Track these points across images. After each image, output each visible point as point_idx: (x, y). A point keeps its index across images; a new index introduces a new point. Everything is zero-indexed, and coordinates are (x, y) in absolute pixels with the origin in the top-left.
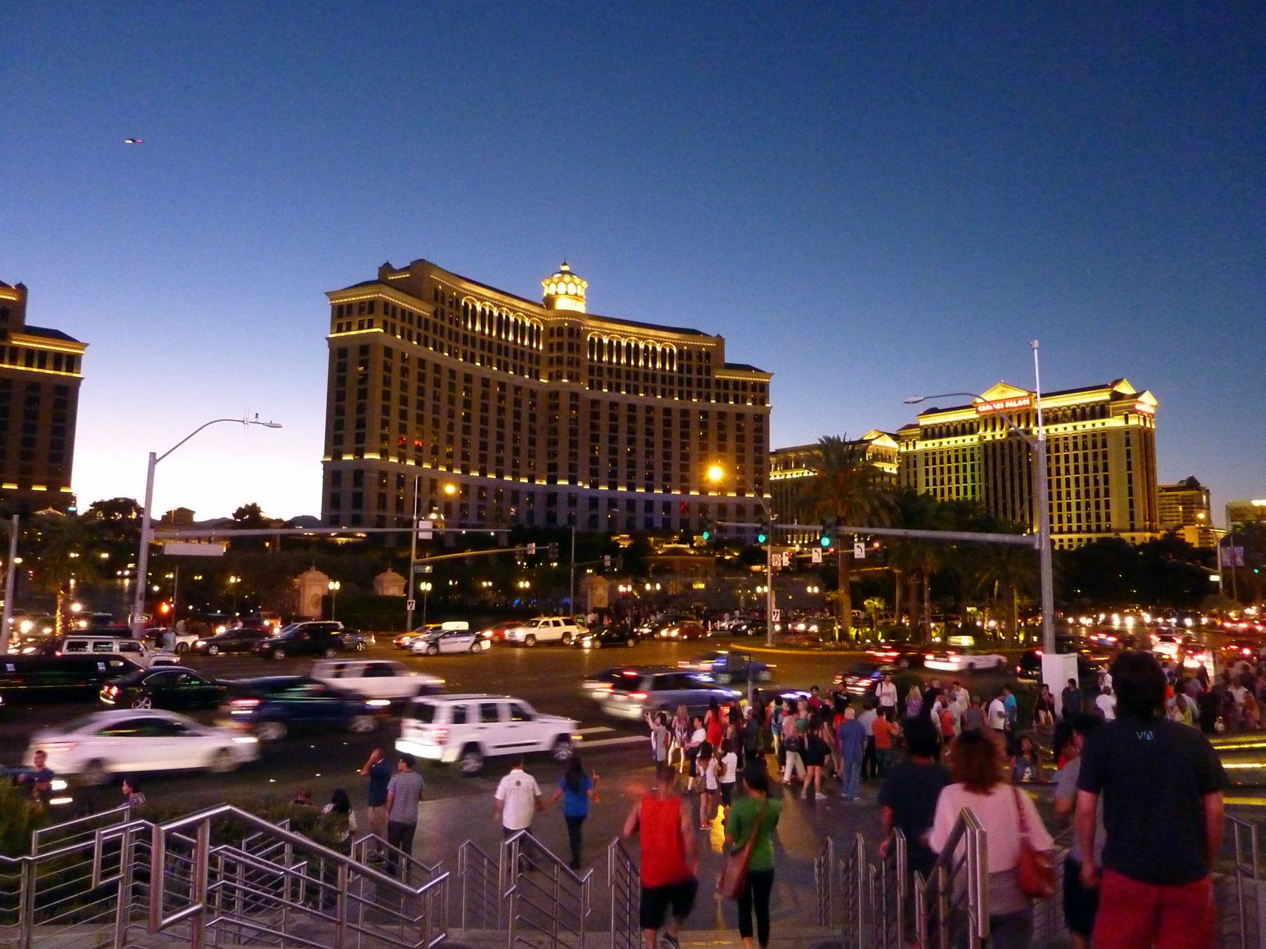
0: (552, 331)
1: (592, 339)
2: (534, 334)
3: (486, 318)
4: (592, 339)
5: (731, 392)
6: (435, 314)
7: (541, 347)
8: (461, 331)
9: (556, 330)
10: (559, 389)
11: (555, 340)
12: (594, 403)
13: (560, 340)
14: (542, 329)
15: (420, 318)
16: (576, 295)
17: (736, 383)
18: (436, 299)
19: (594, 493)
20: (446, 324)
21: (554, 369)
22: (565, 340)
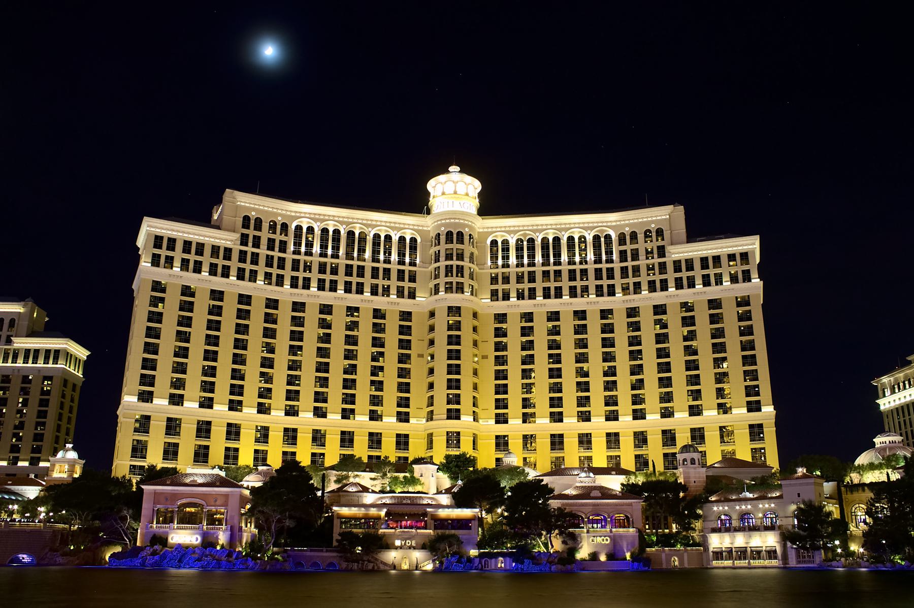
1: (494, 243)
2: (409, 246)
3: (330, 238)
4: (494, 243)
5: (698, 273)
6: (244, 240)
7: (418, 262)
8: (289, 256)
9: (434, 237)
10: (436, 306)
11: (434, 249)
12: (501, 318)
13: (437, 248)
14: (419, 240)
15: (215, 250)
16: (455, 193)
17: (704, 262)
18: (246, 225)
20: (263, 251)
21: (431, 285)
22: (443, 247)
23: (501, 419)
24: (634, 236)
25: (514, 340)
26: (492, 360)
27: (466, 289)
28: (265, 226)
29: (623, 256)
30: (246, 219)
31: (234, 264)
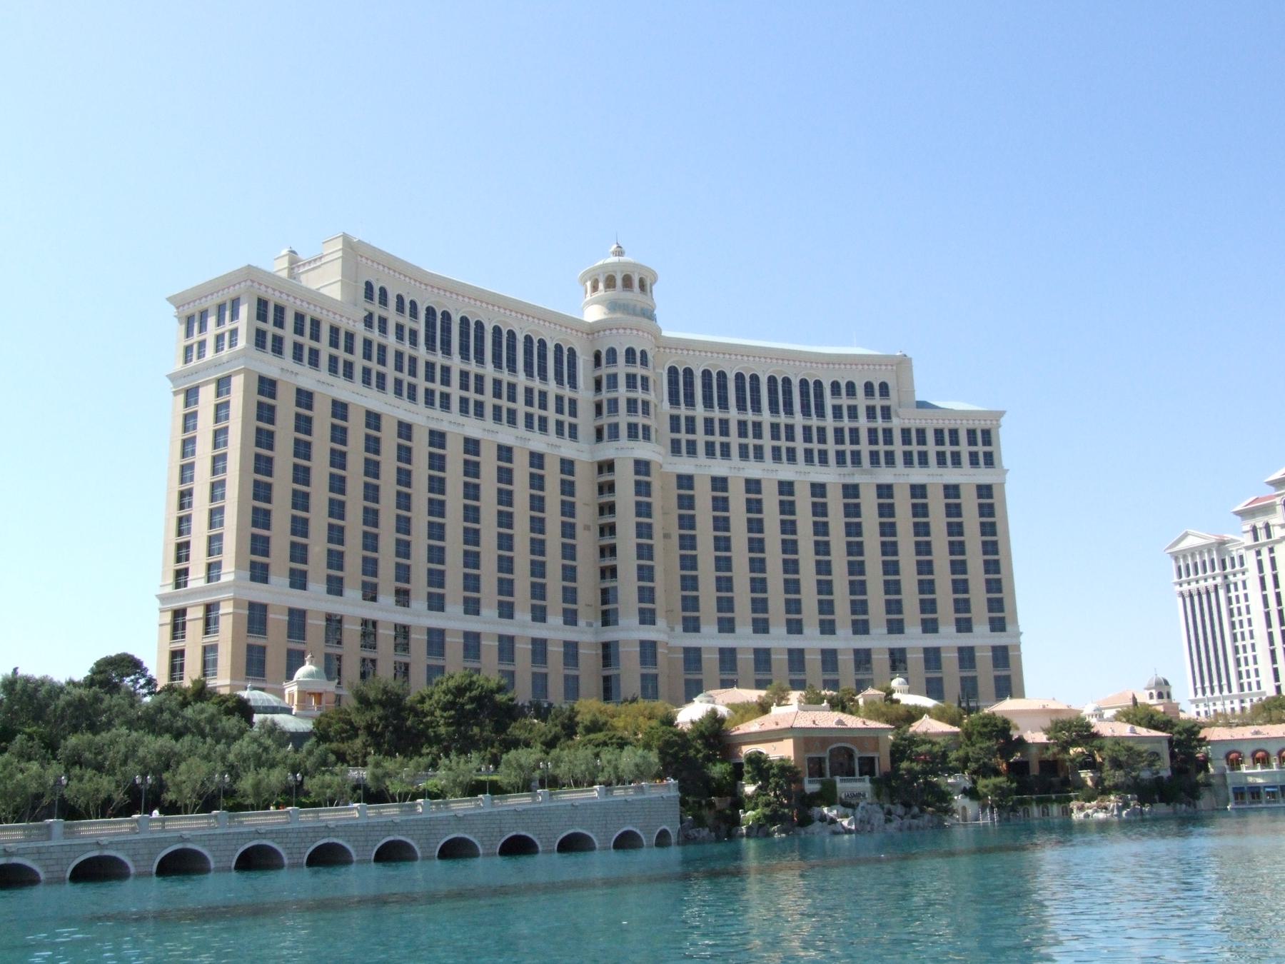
0: (597, 356)
1: (673, 371)
6: (368, 321)
12: (685, 481)
14: (578, 354)
15: (334, 331)
19: (692, 640)
20: (391, 340)
22: (622, 369)
23: (692, 625)
24: (851, 387)
25: (704, 513)
26: (675, 540)
27: (653, 436)
28: (392, 302)
29: (837, 411)
30: (369, 287)
31: (358, 359)
